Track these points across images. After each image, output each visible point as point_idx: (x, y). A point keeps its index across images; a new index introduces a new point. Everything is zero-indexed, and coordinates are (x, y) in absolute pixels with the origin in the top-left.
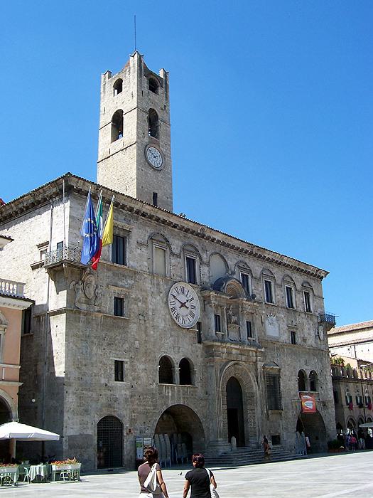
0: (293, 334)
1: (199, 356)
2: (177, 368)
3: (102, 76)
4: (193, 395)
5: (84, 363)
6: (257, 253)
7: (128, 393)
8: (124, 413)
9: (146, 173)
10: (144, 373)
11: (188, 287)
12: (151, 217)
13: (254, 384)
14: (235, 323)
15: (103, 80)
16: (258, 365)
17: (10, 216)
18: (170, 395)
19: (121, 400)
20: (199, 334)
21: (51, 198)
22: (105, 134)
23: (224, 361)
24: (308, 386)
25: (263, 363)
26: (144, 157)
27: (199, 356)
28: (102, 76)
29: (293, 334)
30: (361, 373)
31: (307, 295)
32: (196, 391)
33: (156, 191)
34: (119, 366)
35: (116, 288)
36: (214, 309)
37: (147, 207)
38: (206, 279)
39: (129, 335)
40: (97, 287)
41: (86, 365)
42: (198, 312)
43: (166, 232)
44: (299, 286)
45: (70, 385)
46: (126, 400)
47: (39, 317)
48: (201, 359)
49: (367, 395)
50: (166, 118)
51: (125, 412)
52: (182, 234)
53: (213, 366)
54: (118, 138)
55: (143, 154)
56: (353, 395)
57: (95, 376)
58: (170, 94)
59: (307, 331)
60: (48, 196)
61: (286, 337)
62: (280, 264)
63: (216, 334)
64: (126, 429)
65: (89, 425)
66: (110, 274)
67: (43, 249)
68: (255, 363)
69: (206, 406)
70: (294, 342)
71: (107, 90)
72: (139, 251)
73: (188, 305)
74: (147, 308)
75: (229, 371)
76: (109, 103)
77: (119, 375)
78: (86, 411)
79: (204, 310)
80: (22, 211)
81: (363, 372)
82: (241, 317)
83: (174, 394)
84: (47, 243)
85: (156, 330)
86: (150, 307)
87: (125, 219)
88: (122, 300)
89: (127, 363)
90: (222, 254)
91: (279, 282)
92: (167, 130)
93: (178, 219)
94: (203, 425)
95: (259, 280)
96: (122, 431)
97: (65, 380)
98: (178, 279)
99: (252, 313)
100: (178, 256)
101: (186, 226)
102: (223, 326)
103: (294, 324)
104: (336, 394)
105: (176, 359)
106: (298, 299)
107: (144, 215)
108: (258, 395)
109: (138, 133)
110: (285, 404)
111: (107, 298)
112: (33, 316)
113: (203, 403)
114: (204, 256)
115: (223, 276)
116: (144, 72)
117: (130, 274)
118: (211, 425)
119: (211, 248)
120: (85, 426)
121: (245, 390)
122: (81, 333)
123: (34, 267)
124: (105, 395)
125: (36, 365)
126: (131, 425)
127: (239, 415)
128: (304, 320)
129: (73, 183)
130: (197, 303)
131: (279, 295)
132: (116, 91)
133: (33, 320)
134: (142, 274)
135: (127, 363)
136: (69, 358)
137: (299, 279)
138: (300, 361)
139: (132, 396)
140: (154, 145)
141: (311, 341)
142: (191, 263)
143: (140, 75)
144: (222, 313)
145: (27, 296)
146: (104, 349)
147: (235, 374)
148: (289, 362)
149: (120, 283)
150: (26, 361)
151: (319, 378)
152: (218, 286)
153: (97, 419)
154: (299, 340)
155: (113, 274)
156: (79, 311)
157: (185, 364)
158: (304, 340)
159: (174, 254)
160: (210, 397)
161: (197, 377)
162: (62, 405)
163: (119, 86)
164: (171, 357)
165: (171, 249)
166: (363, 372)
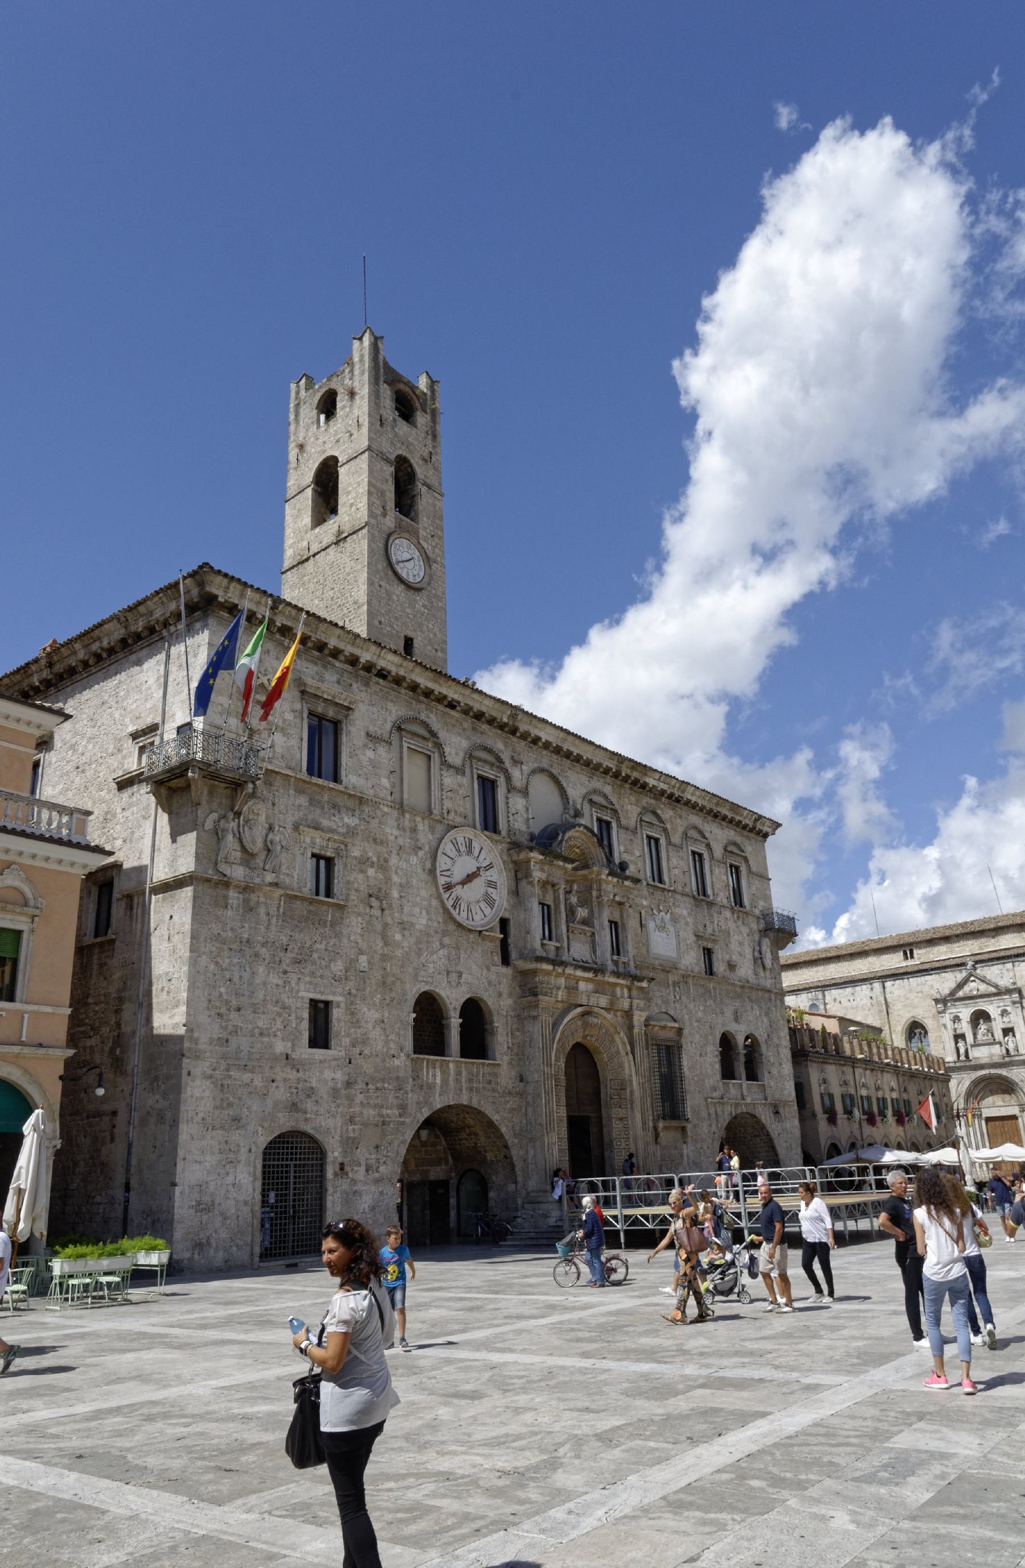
0: (708, 953)
1: (505, 995)
2: (455, 1022)
3: (293, 386)
5: (234, 1003)
7: (340, 1076)
8: (327, 1124)
9: (389, 594)
10: (377, 1028)
11: (481, 840)
12: (398, 681)
13: (628, 1062)
14: (585, 922)
15: (293, 395)
16: (636, 1018)
17: (72, 671)
18: (438, 1081)
19: (323, 1092)
20: (504, 945)
21: (166, 624)
22: (298, 513)
23: (560, 1006)
24: (741, 1069)
25: (645, 1015)
26: (383, 558)
27: (505, 995)
28: (293, 386)
29: (708, 953)
30: (851, 1043)
31: (735, 870)
33: (411, 634)
34: (320, 1013)
35: (316, 834)
36: (537, 890)
37: (391, 657)
38: (519, 825)
39: (345, 940)
40: (271, 828)
41: (239, 1010)
42: (501, 896)
44: (718, 851)
45: (197, 1057)
46: (335, 1093)
47: (129, 897)
48: (510, 1002)
49: (864, 1092)
50: (433, 481)
51: (331, 1123)
53: (535, 1018)
54: (325, 521)
55: (382, 552)
56: (837, 1091)
57: (261, 1034)
58: (440, 428)
59: (738, 945)
60: (158, 622)
61: (692, 960)
62: (678, 800)
63: (543, 945)
64: (334, 1162)
65: (243, 1156)
66: (303, 800)
67: (144, 741)
68: (628, 1014)
69: (521, 1107)
70: (710, 971)
71: (302, 416)
72: (370, 754)
73: (478, 875)
74: (388, 880)
76: (313, 440)
77: (320, 1037)
78: (237, 1119)
79: (516, 892)
80: (98, 658)
81: (855, 1041)
82: (596, 910)
83: (449, 1082)
84: (153, 728)
85: (407, 933)
86: (395, 879)
87: (338, 682)
88: (329, 862)
89: (338, 1006)
90: (555, 771)
91: (676, 839)
92: (435, 506)
93: (460, 689)
94: (514, 1152)
95: (634, 832)
96: (322, 1168)
97: (187, 1044)
98: (459, 820)
99: (620, 904)
100: (459, 771)
101: (476, 707)
102: (556, 925)
103: (709, 930)
104: (801, 1089)
105: (453, 998)
106: (718, 880)
107: (382, 674)
109: (370, 505)
110: (692, 1108)
111: (294, 856)
112: (116, 895)
113: (513, 1103)
114: (516, 774)
115: (559, 822)
116: (384, 374)
117: (350, 803)
118: (531, 1152)
119: (532, 759)
120: (231, 1156)
121: (607, 1075)
122: (230, 934)
123: (124, 784)
124: (285, 1080)
125: (118, 1011)
126: (345, 1153)
127: (593, 1130)
128: (731, 925)
129: (216, 588)
130: (500, 875)
131: (677, 866)
132: (322, 417)
133: (111, 900)
134: (376, 805)
135: (338, 1006)
136: (197, 992)
137: (719, 835)
138: (722, 1013)
139: (348, 1084)
140: (407, 535)
141: (746, 970)
142: (487, 786)
143: (375, 380)
144: (556, 899)
145: (94, 837)
146: (285, 972)
147: (585, 1037)
148: (700, 1014)
149: (325, 823)
150: (96, 1004)
151: (764, 1048)
152: (546, 841)
153: (263, 1140)
154: (720, 967)
155: (311, 801)
156: (226, 883)
157: (474, 1012)
158: (732, 967)
159: (450, 766)
160: (530, 1089)
161: (502, 1039)
162: (176, 1106)
163: (328, 406)
164: (443, 994)
165: (442, 755)
166: (855, 1041)
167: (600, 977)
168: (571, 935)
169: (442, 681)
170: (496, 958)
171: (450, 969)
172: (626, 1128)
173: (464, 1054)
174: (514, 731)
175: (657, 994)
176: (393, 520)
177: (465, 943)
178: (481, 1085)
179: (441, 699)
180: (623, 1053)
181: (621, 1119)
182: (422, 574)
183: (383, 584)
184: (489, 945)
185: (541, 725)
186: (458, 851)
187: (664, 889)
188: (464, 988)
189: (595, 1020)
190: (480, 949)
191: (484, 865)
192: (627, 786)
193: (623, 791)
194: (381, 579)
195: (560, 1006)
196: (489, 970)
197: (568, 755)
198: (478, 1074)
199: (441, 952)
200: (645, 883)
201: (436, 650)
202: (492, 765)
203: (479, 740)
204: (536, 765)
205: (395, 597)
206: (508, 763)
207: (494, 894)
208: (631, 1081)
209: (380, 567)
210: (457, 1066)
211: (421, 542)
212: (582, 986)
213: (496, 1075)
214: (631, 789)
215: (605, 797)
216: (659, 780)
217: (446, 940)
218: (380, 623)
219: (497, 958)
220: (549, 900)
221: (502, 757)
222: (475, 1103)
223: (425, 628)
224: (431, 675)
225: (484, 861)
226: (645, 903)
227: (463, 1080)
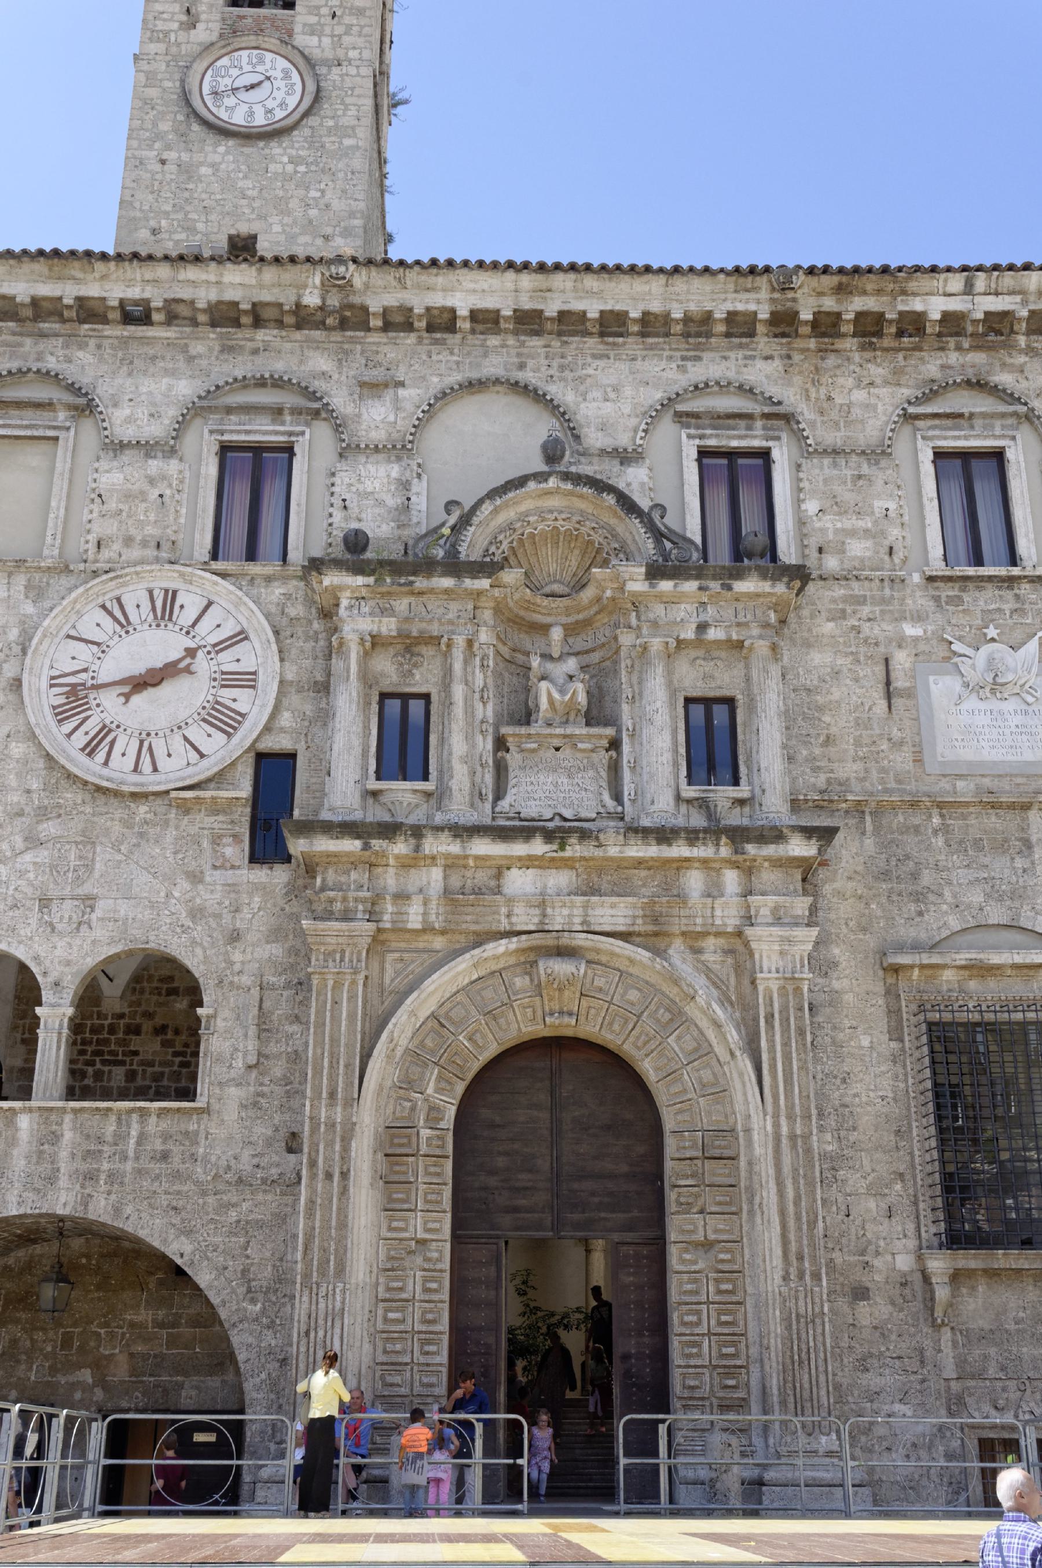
1: (251, 937)
2: (55, 1015)
4: (165, 1156)
6: (848, 313)
9: (187, 170)
32: (192, 1138)
33: (244, 228)
43: (85, 361)
52: (205, 343)
75: (457, 1002)
90: (528, 376)
94: (241, 1340)
98: (136, 553)
99: (740, 645)
100: (167, 448)
101: (205, 297)
102: (442, 740)
108: (761, 1148)
119: (425, 369)
140: (252, 41)
159: (120, 447)
161: (226, 1041)
167: (575, 849)
168: (513, 758)
169: (75, 269)
170: (229, 851)
171: (50, 894)
172: (731, 1275)
173: (70, 1093)
174: (352, 319)
175: (963, 875)
176: (216, 27)
177: (117, 828)
178: (129, 1166)
179: (89, 312)
180: (719, 1050)
181: (707, 1245)
182: (292, 101)
183: (171, 155)
184: (205, 822)
185: (440, 279)
186: (125, 624)
187: (1011, 581)
188: (100, 933)
189: (562, 968)
190: (171, 834)
191: (213, 639)
192: (850, 344)
193: (831, 361)
194: (168, 147)
195: (439, 943)
196: (196, 878)
197: (570, 323)
198: (120, 1137)
199: (28, 857)
200: (916, 578)
201: (326, 238)
202: (277, 412)
203: (241, 367)
204: (455, 378)
205: (204, 170)
206: (340, 400)
207: (242, 699)
208: (748, 1131)
209: (165, 126)
210: (47, 1122)
211: (301, 40)
212: (520, 882)
213: (192, 1138)
214: (863, 348)
215: (747, 391)
216: (969, 289)
217: (49, 828)
218: (154, 232)
219: (237, 851)
220: (424, 680)
221: (319, 385)
222: (100, 1210)
223: (294, 204)
224: (40, 267)
225: (208, 632)
226: (911, 630)
227: (64, 1154)
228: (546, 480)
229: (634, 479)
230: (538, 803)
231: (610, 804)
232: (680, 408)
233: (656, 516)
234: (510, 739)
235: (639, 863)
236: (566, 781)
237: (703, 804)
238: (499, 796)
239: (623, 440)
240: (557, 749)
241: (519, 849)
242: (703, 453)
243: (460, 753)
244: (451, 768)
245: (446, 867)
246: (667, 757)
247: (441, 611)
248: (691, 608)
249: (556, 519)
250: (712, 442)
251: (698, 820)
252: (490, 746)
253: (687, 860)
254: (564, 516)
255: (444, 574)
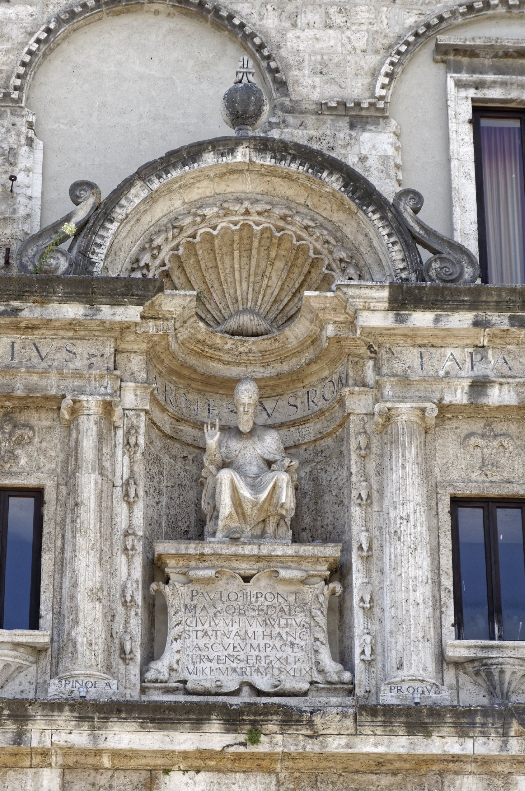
102: (61, 564)
167: (273, 741)
168: (176, 594)
228: (232, 151)
229: (372, 151)
230: (214, 665)
231: (331, 666)
232: (444, 39)
233: (406, 208)
234: (171, 562)
235: (379, 764)
236: (260, 630)
237: (481, 669)
238: (152, 652)
239: (356, 89)
240: (247, 579)
241: (184, 740)
242: (481, 111)
243: (90, 584)
244: (74, 610)
245: (66, 769)
246: (423, 593)
247: (62, 355)
248: (462, 354)
249: (247, 213)
250: (495, 94)
251: (473, 695)
252: (138, 573)
253: (456, 759)
254: (259, 208)
255: (67, 298)
